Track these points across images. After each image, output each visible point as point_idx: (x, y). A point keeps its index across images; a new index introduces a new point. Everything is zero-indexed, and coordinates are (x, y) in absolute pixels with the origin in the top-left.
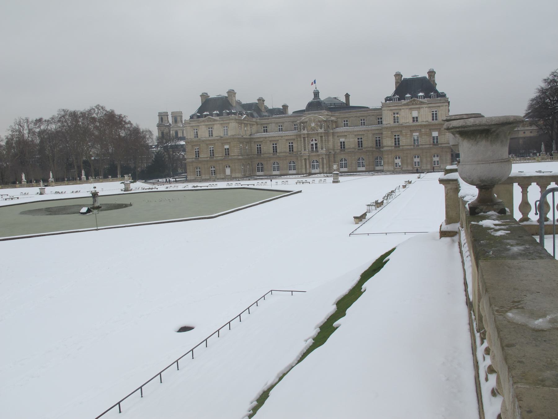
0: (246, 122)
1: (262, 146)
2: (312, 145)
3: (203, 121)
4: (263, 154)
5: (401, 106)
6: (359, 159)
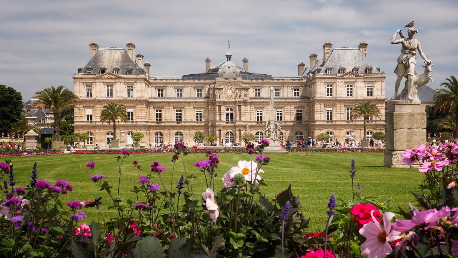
1: (163, 113)
2: (227, 115)
3: (101, 77)
4: (164, 122)
5: (336, 78)
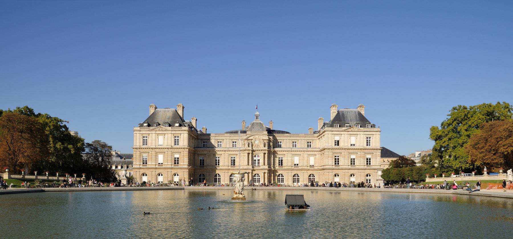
2: (255, 160)
6: (294, 176)
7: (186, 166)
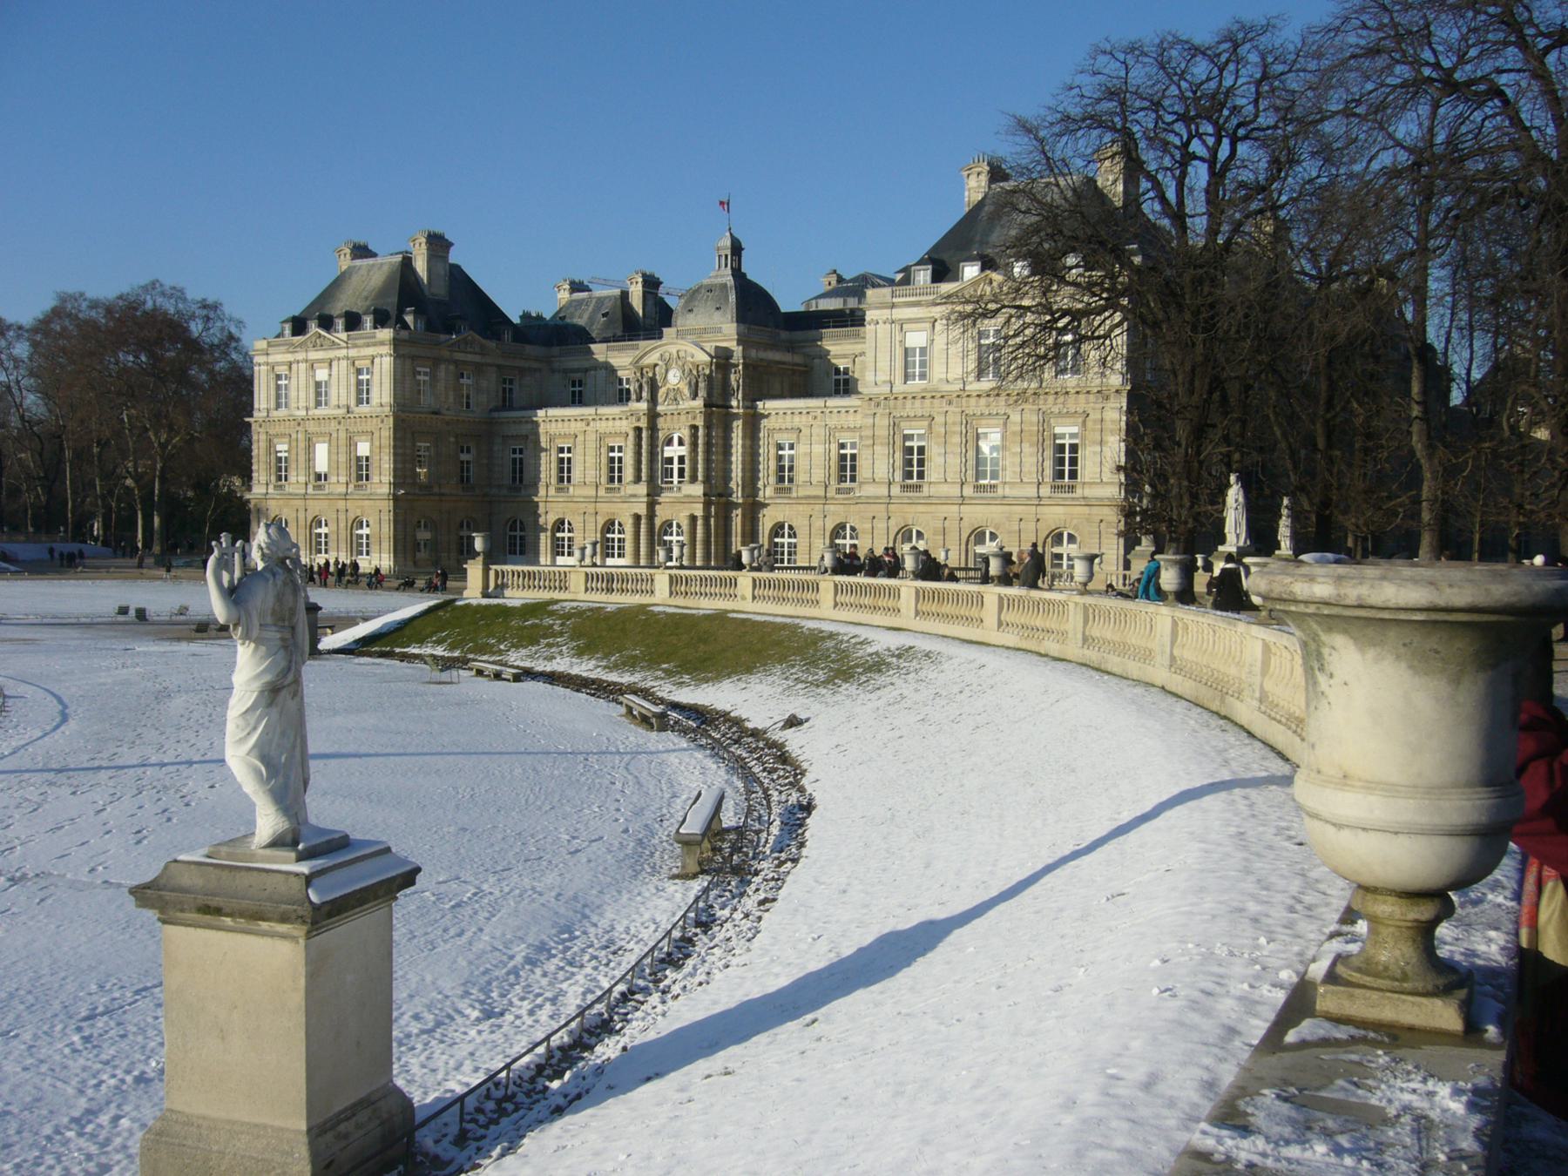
0: (477, 359)
7: (385, 490)
